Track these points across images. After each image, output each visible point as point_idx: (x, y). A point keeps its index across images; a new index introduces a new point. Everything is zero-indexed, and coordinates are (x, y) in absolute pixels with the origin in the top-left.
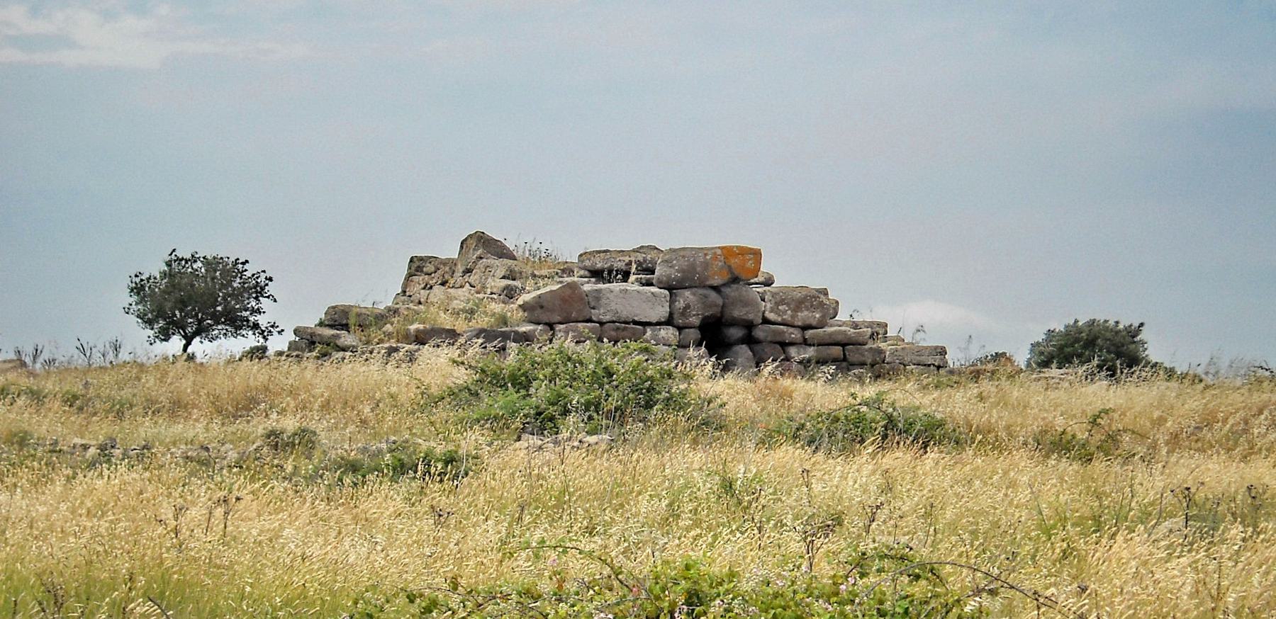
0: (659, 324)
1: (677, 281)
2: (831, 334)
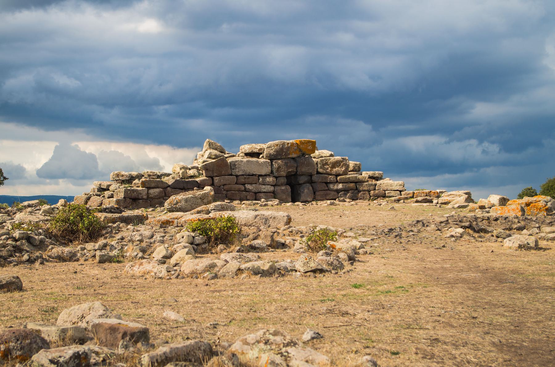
0: (266, 175)
1: (274, 156)
2: (349, 178)
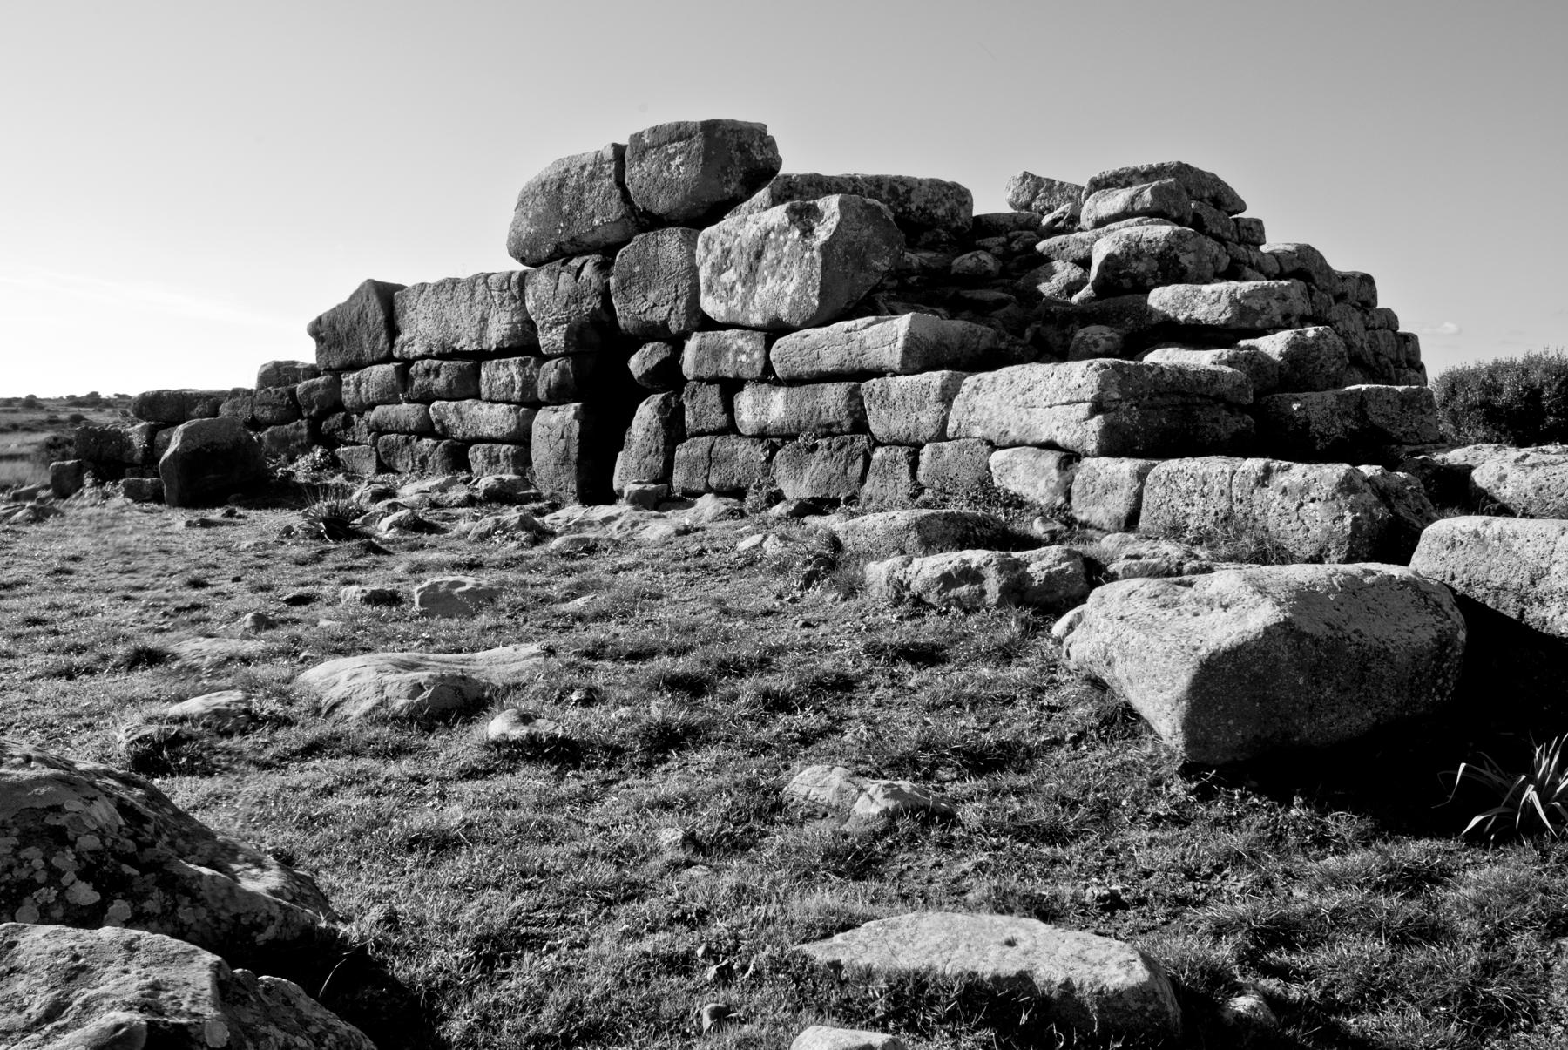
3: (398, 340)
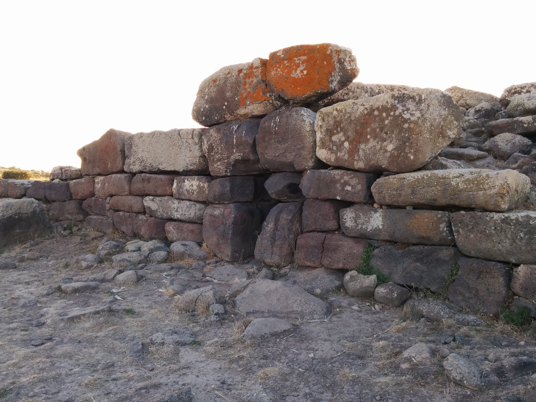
0: (187, 173)
2: (414, 187)
3: (127, 161)
